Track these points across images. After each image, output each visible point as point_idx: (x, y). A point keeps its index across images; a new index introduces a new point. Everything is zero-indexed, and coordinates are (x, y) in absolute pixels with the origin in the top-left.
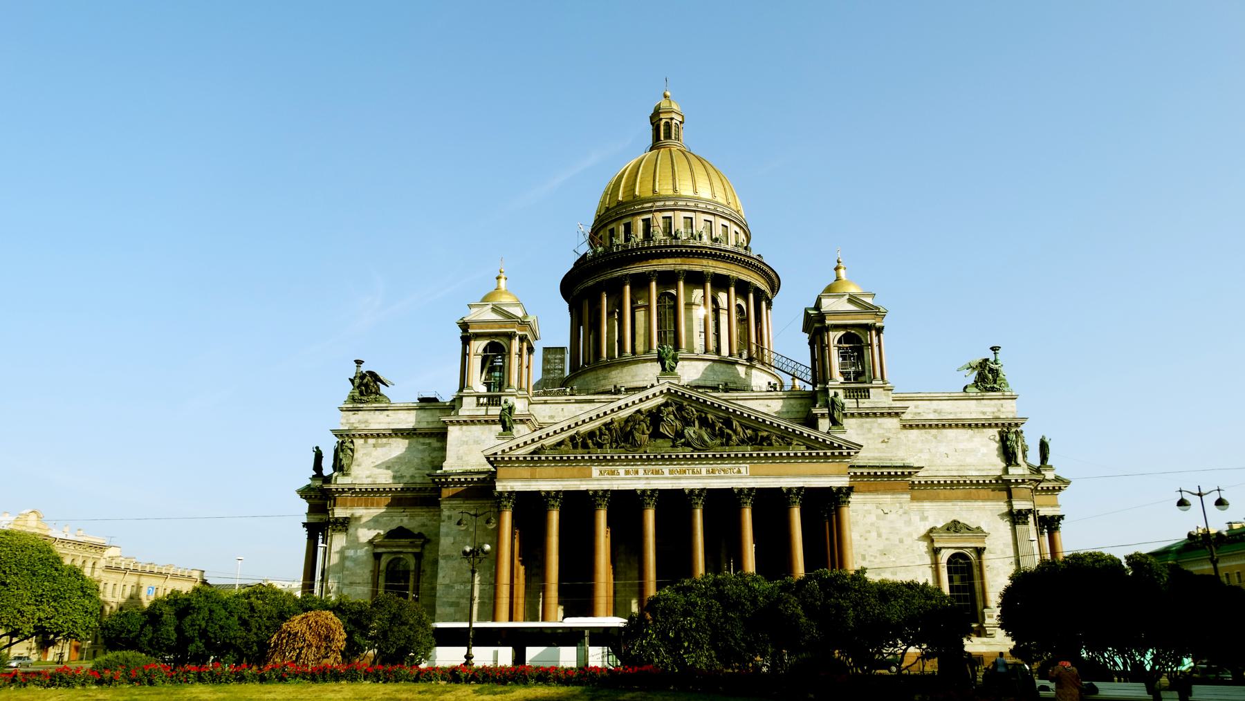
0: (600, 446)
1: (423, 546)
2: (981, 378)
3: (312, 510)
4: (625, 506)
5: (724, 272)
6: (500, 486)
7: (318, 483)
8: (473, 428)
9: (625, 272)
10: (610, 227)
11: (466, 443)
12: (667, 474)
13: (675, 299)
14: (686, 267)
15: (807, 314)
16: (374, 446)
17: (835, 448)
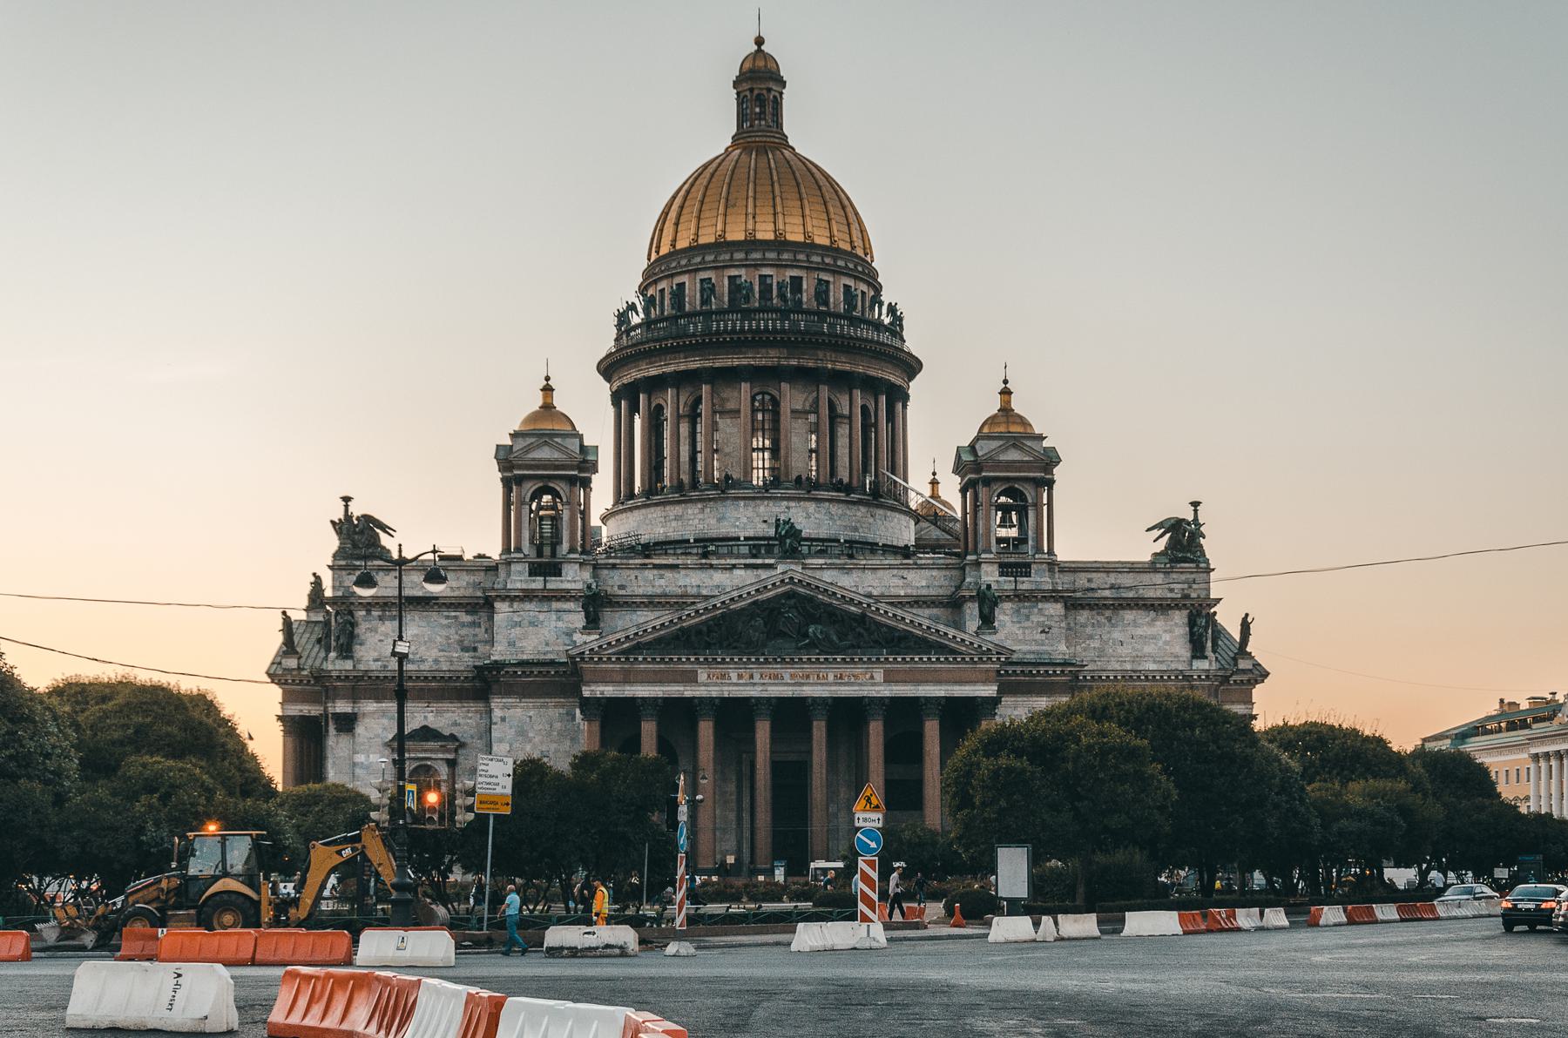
0: (708, 646)
1: (456, 751)
2: (1172, 545)
3: (287, 699)
4: (734, 716)
5: (847, 367)
6: (586, 692)
7: (292, 663)
8: (528, 606)
9: (708, 364)
10: (678, 280)
11: (518, 624)
12: (787, 679)
13: (776, 403)
14: (794, 362)
15: (958, 456)
16: (381, 618)
17: (983, 653)
